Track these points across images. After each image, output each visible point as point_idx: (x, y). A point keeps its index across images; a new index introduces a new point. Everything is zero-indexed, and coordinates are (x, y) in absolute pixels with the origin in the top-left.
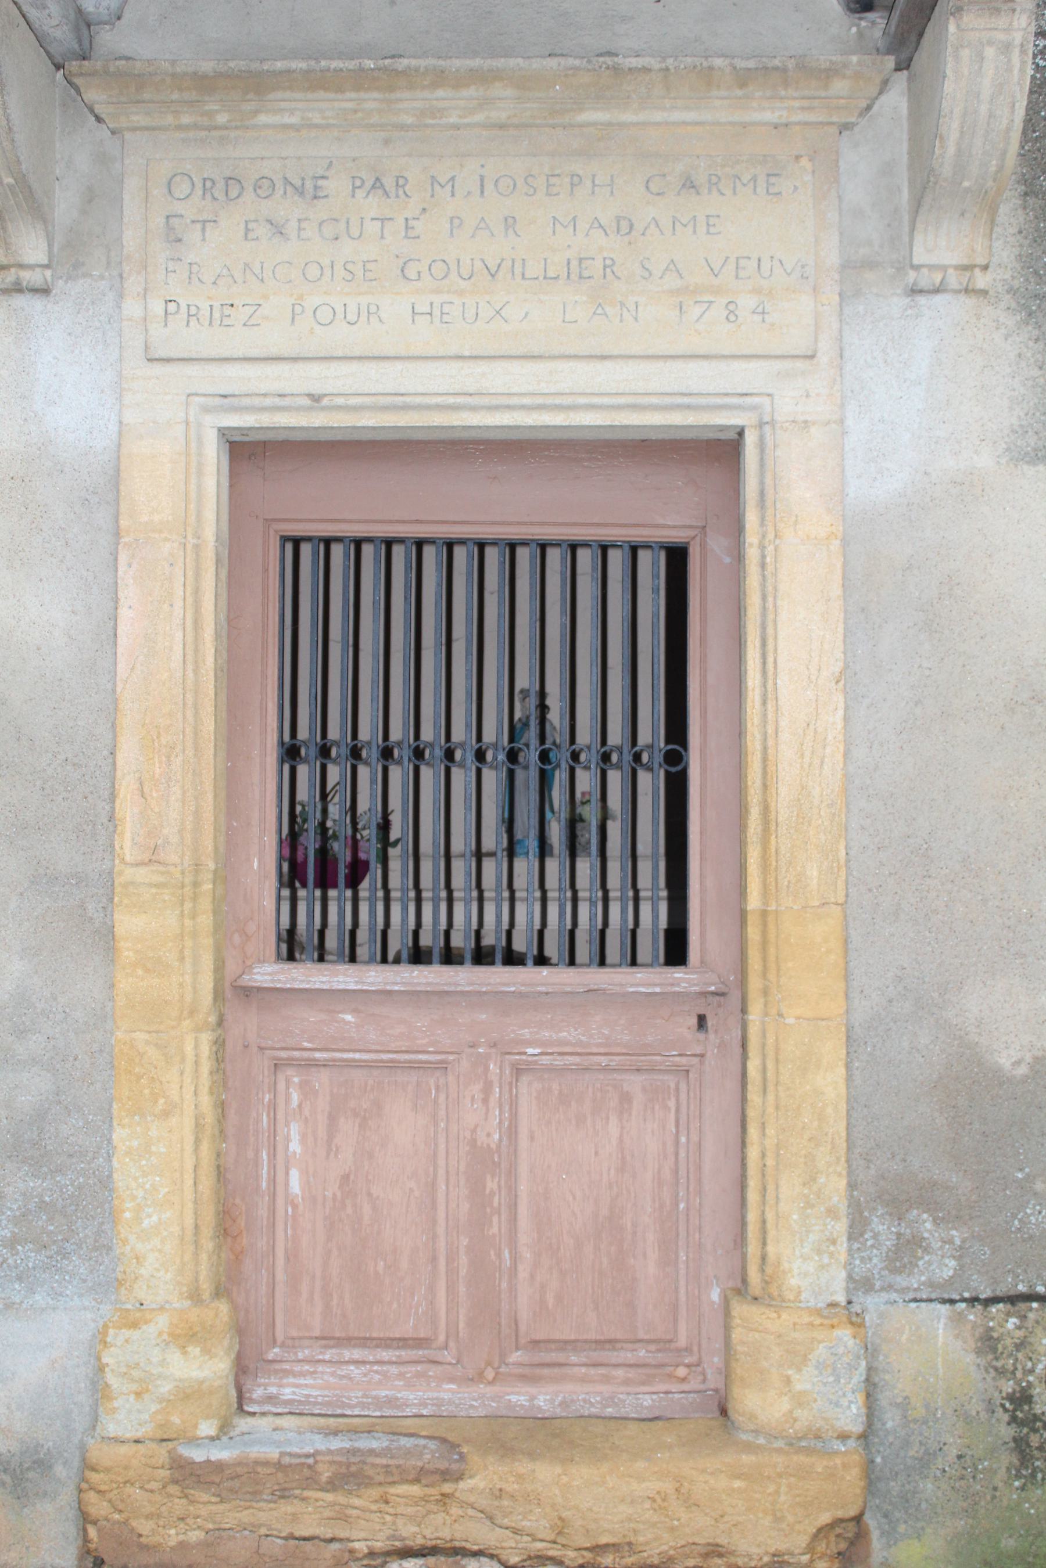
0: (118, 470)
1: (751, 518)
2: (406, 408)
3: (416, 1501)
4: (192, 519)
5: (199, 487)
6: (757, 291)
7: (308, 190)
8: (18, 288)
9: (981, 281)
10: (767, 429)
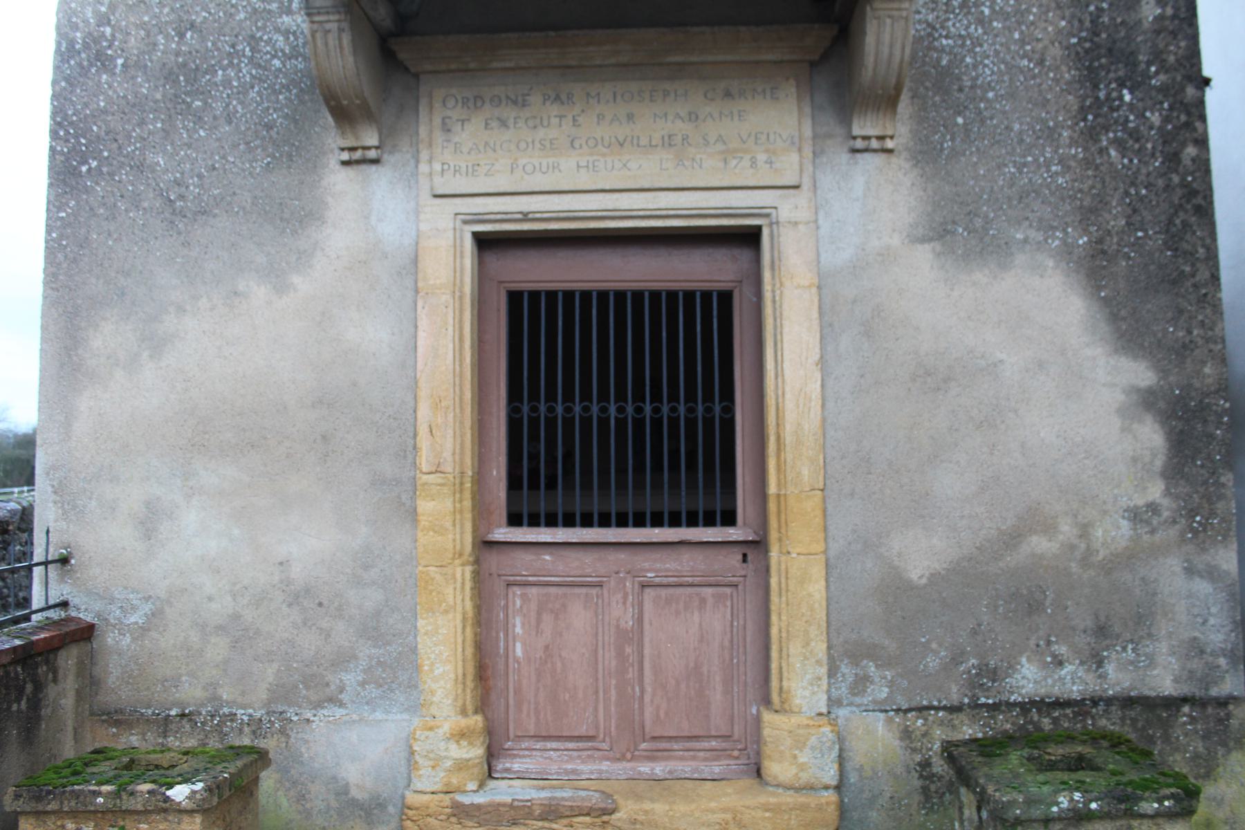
0: (416, 256)
1: (767, 275)
4: (458, 282)
5: (462, 264)
6: (767, 151)
10: (775, 226)
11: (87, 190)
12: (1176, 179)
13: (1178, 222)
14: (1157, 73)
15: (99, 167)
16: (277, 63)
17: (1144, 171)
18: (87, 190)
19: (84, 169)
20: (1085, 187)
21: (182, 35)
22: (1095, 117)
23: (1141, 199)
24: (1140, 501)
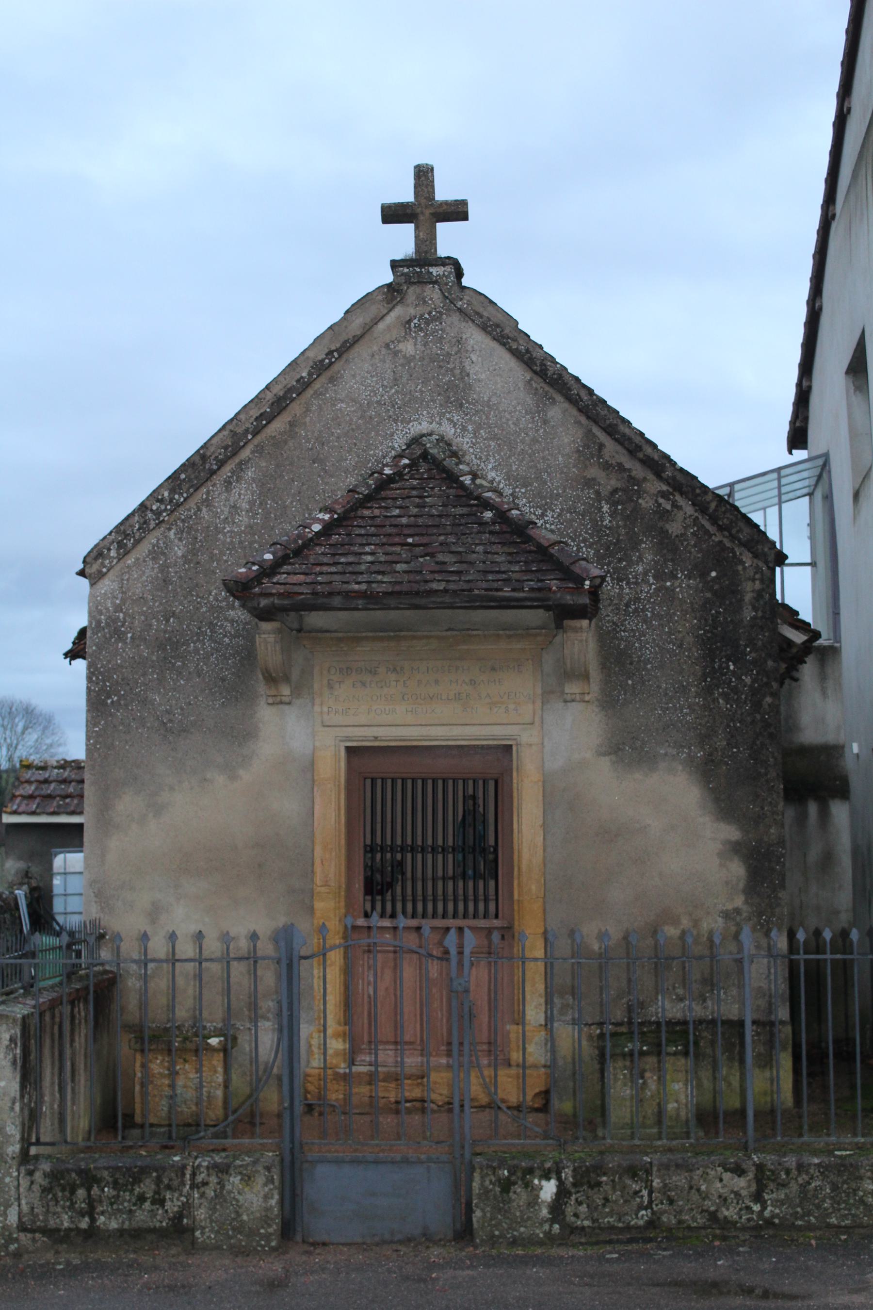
0: (313, 760)
2: (404, 740)
3: (410, 1085)
7: (373, 672)
8: (281, 703)
9: (587, 698)
11: (111, 715)
12: (758, 717)
13: (758, 742)
14: (750, 652)
15: (119, 700)
16: (227, 640)
17: (739, 712)
18: (111, 715)
19: (109, 701)
20: (703, 722)
21: (167, 621)
22: (712, 679)
23: (737, 729)
24: (729, 907)
